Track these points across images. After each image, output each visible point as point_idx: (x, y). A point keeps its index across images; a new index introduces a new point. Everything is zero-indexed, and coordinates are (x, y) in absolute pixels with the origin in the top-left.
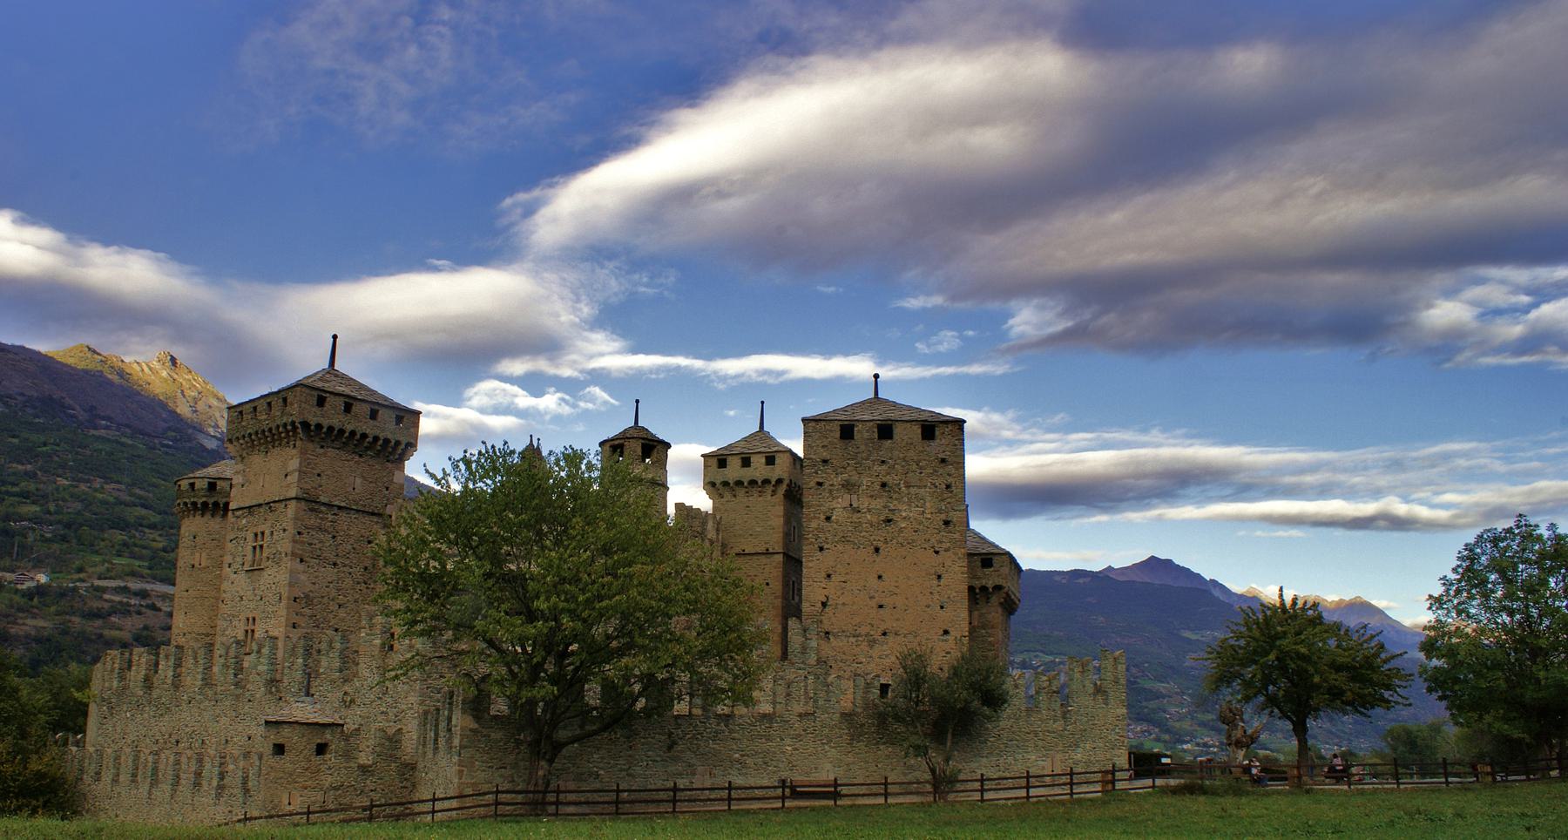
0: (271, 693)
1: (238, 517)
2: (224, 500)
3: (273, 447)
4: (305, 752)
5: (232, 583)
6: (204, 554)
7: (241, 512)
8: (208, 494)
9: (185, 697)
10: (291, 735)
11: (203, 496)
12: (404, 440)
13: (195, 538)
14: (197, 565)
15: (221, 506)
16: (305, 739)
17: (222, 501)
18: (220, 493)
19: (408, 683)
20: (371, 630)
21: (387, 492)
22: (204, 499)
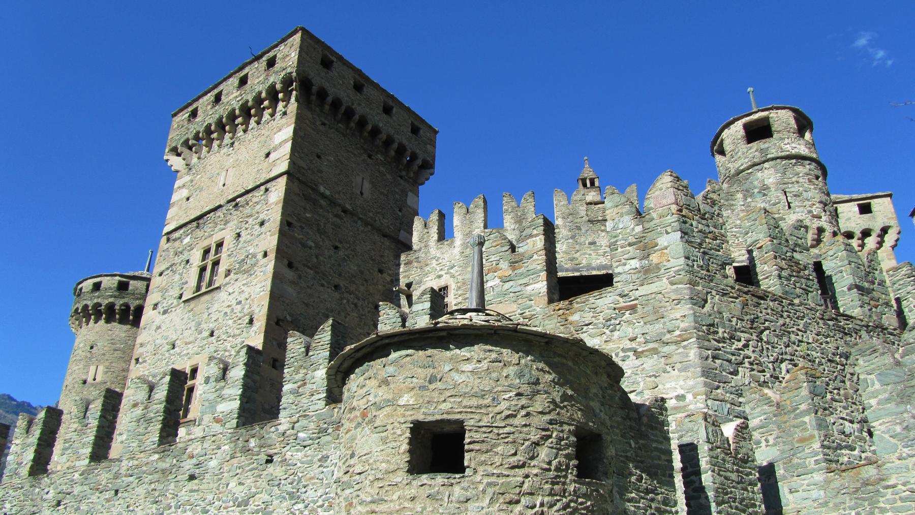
0: (246, 451)
1: (175, 240)
2: (137, 302)
3: (245, 131)
4: (544, 453)
5: (159, 327)
6: (101, 368)
7: (182, 231)
8: (117, 293)
9: (51, 495)
10: (487, 384)
11: (111, 296)
12: (421, 156)
13: (92, 348)
14: (90, 380)
15: (132, 308)
16: (540, 403)
17: (133, 305)
18: (133, 294)
19: (655, 351)
20: (514, 269)
21: (400, 214)
22: (111, 300)
